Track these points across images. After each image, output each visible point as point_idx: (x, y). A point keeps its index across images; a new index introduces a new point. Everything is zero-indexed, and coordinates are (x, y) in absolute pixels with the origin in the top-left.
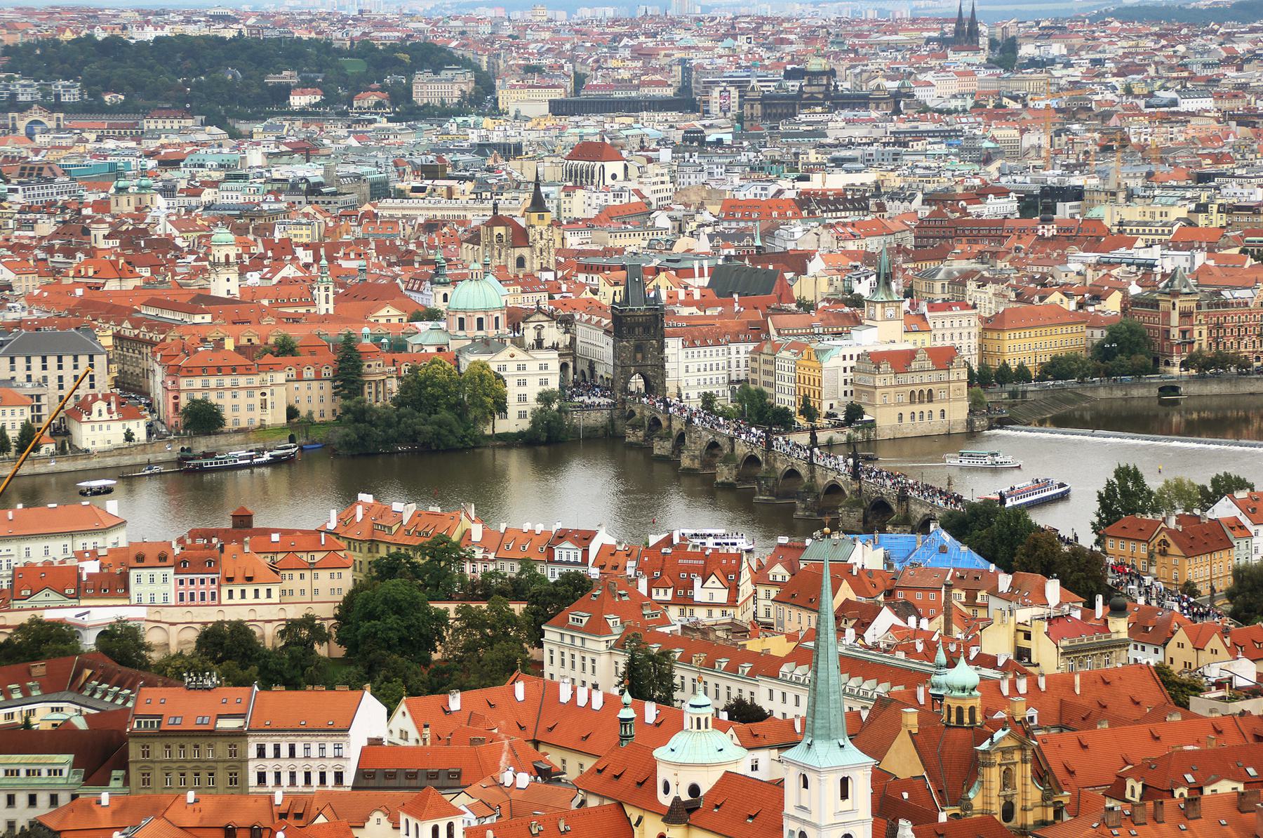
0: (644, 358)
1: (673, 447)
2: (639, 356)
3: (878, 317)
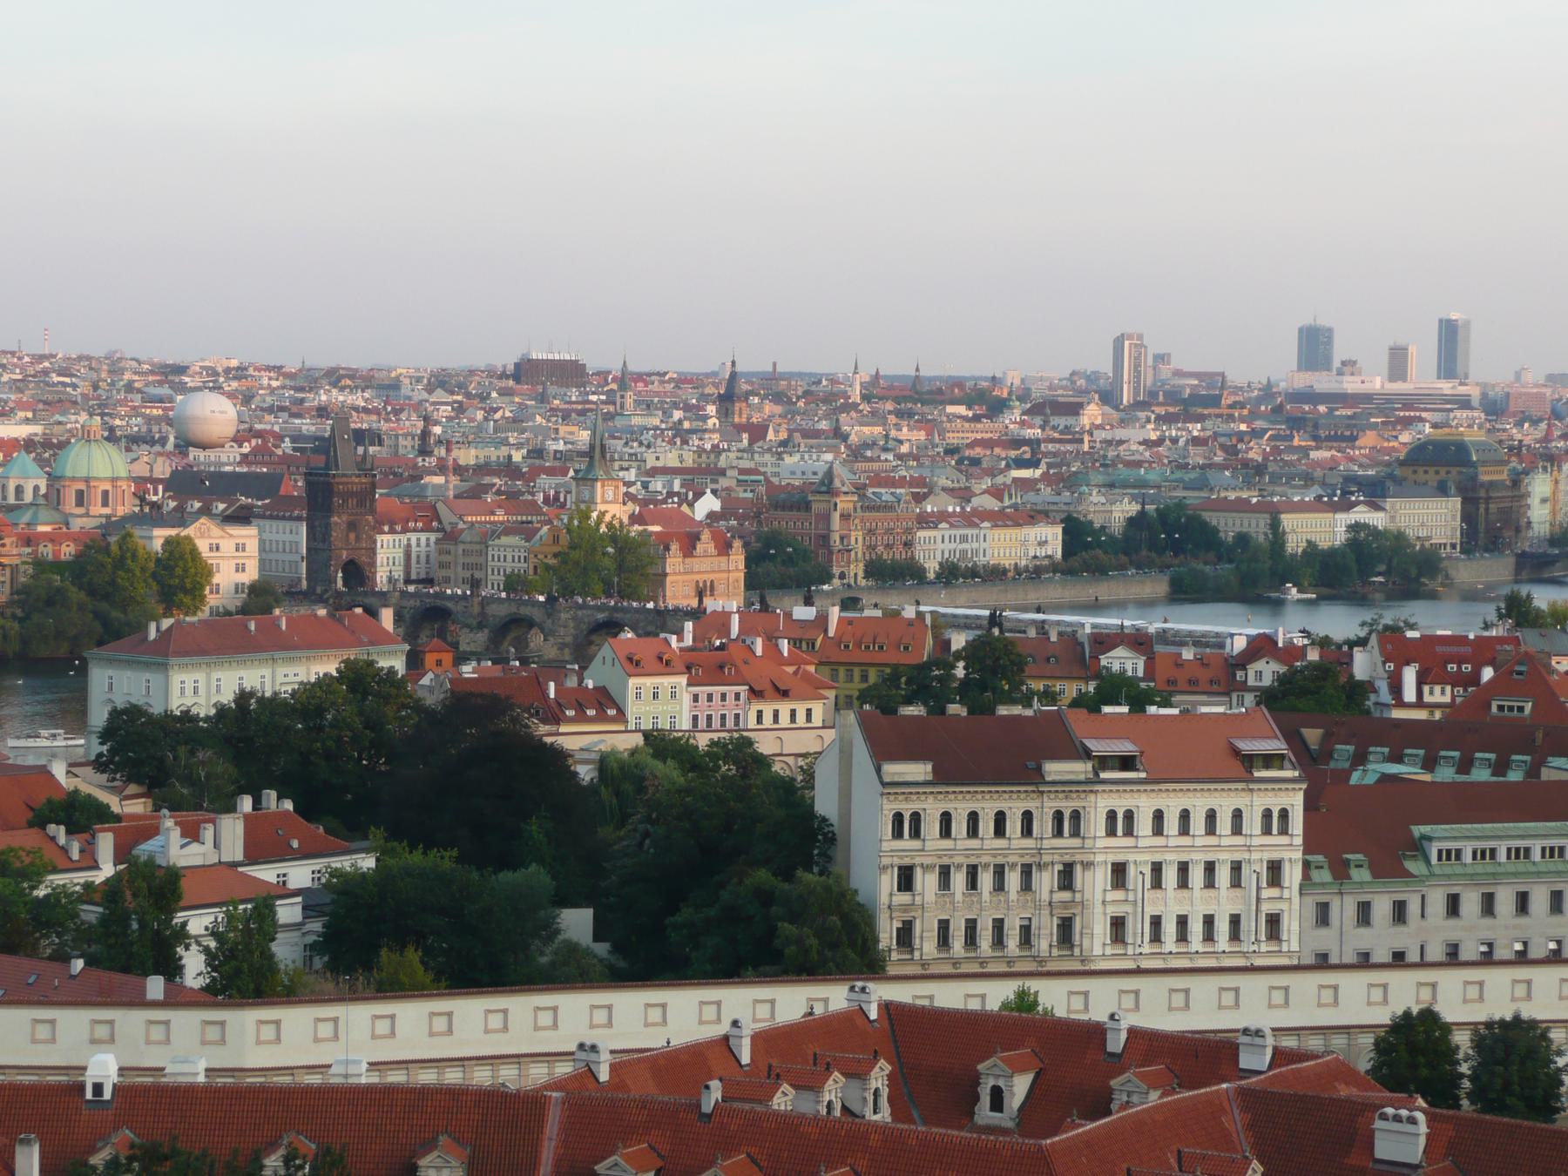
0: (358, 539)
1: (490, 639)
2: (352, 536)
3: (599, 501)
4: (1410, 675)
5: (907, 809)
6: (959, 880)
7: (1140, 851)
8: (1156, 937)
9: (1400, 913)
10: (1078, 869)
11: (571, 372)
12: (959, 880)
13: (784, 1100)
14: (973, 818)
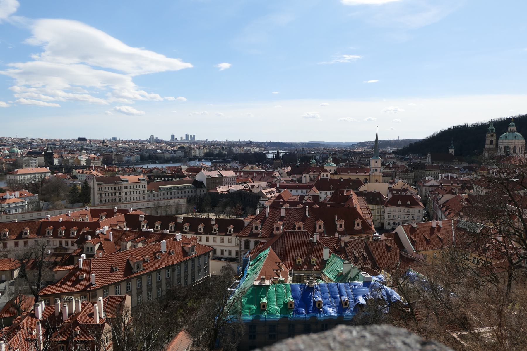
4: (169, 171)
5: (100, 187)
6: (107, 195)
7: (128, 191)
8: (131, 200)
9: (158, 196)
10: (121, 193)
11: (85, 139)
12: (107, 195)
13: (73, 220)
14: (109, 188)
